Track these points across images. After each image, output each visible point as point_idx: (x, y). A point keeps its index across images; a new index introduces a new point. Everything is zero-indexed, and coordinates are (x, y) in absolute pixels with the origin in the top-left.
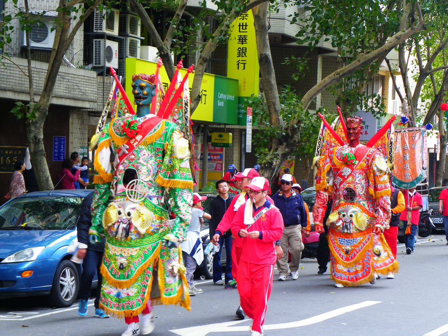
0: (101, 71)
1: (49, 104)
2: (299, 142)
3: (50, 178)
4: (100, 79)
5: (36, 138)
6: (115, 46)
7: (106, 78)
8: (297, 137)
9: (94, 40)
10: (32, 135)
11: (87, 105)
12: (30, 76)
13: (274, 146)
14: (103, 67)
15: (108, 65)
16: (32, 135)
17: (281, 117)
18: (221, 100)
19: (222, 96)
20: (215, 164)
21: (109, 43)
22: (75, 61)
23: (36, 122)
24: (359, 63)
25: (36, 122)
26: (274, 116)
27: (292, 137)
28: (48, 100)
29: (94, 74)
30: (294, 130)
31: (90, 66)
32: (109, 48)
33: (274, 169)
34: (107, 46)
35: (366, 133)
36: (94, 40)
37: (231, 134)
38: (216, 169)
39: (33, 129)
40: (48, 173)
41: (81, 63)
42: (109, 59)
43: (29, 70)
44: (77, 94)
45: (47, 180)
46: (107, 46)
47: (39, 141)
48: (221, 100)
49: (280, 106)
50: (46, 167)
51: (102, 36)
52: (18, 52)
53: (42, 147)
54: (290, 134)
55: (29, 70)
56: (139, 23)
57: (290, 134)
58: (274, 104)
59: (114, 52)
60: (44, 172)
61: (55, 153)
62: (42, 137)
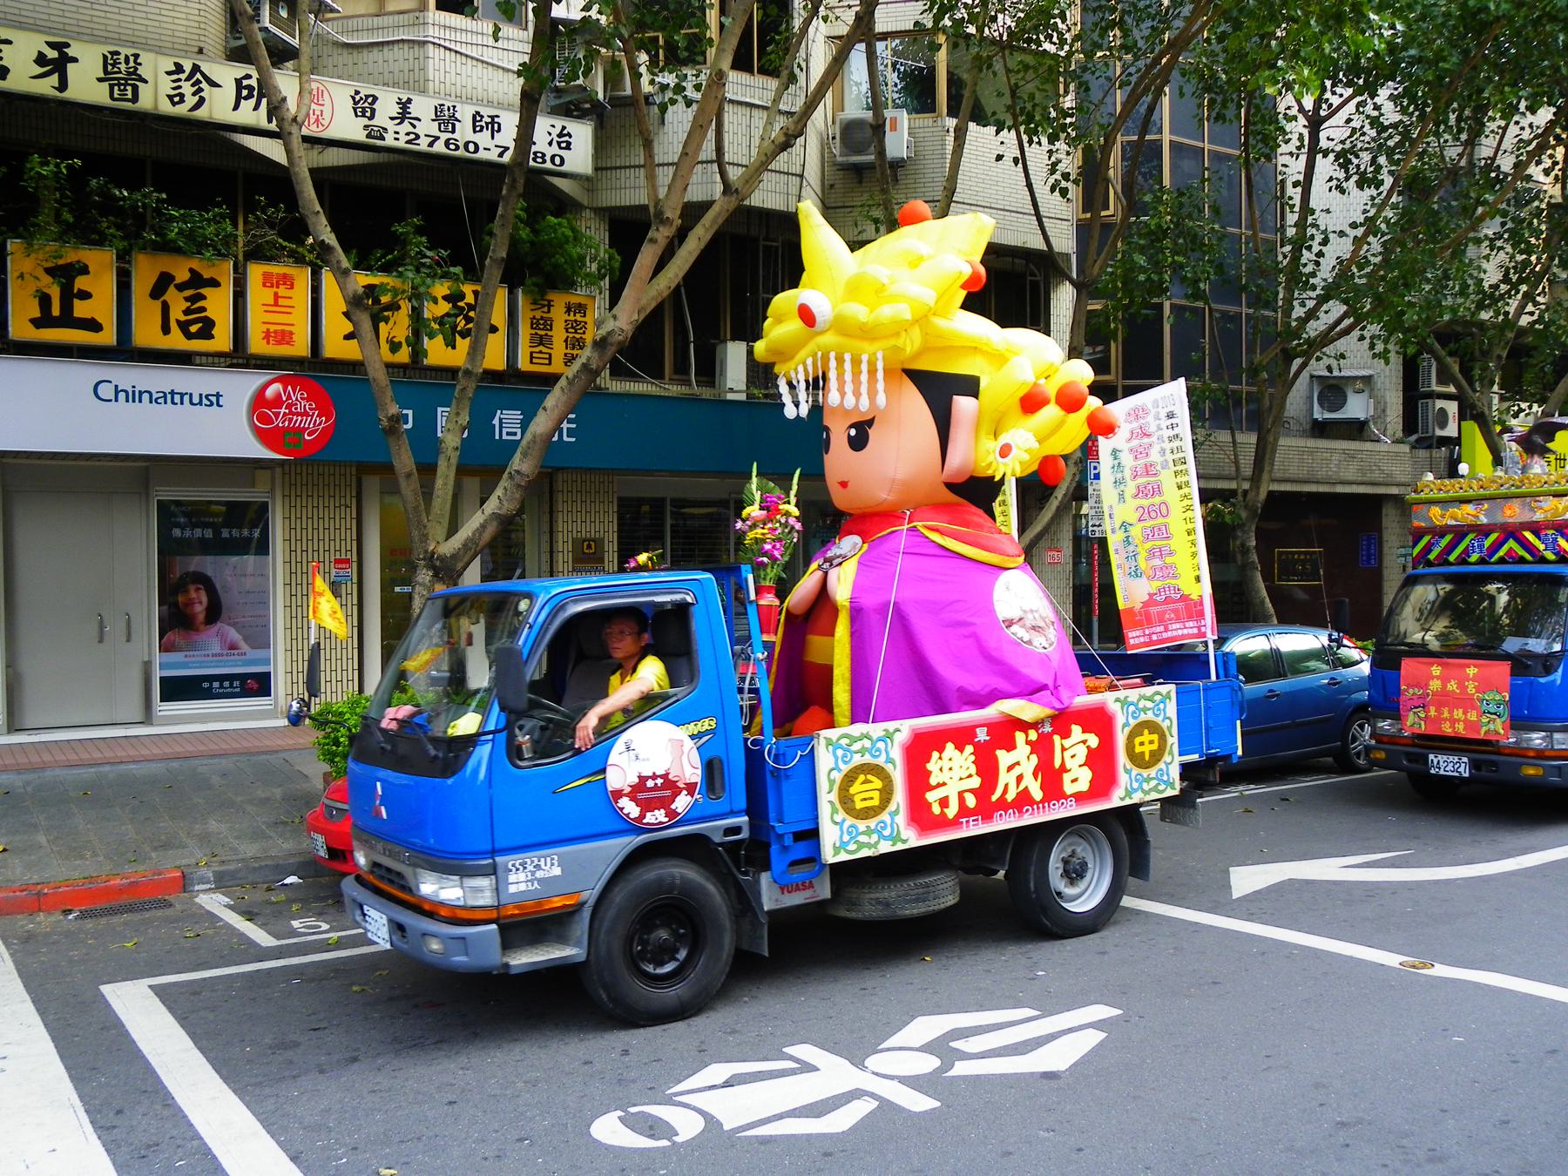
1: (1263, 496)
4: (1422, 453)
5: (1243, 545)
6: (1452, 408)
11: (1394, 491)
12: (1236, 462)
15: (1439, 433)
21: (1440, 404)
22: (1389, 432)
29: (1406, 448)
31: (1413, 438)
32: (1443, 411)
40: (1264, 593)
41: (1400, 434)
42: (1443, 425)
43: (1236, 455)
44: (1376, 476)
45: (1263, 602)
53: (1255, 558)
55: (1236, 455)
60: (1258, 592)
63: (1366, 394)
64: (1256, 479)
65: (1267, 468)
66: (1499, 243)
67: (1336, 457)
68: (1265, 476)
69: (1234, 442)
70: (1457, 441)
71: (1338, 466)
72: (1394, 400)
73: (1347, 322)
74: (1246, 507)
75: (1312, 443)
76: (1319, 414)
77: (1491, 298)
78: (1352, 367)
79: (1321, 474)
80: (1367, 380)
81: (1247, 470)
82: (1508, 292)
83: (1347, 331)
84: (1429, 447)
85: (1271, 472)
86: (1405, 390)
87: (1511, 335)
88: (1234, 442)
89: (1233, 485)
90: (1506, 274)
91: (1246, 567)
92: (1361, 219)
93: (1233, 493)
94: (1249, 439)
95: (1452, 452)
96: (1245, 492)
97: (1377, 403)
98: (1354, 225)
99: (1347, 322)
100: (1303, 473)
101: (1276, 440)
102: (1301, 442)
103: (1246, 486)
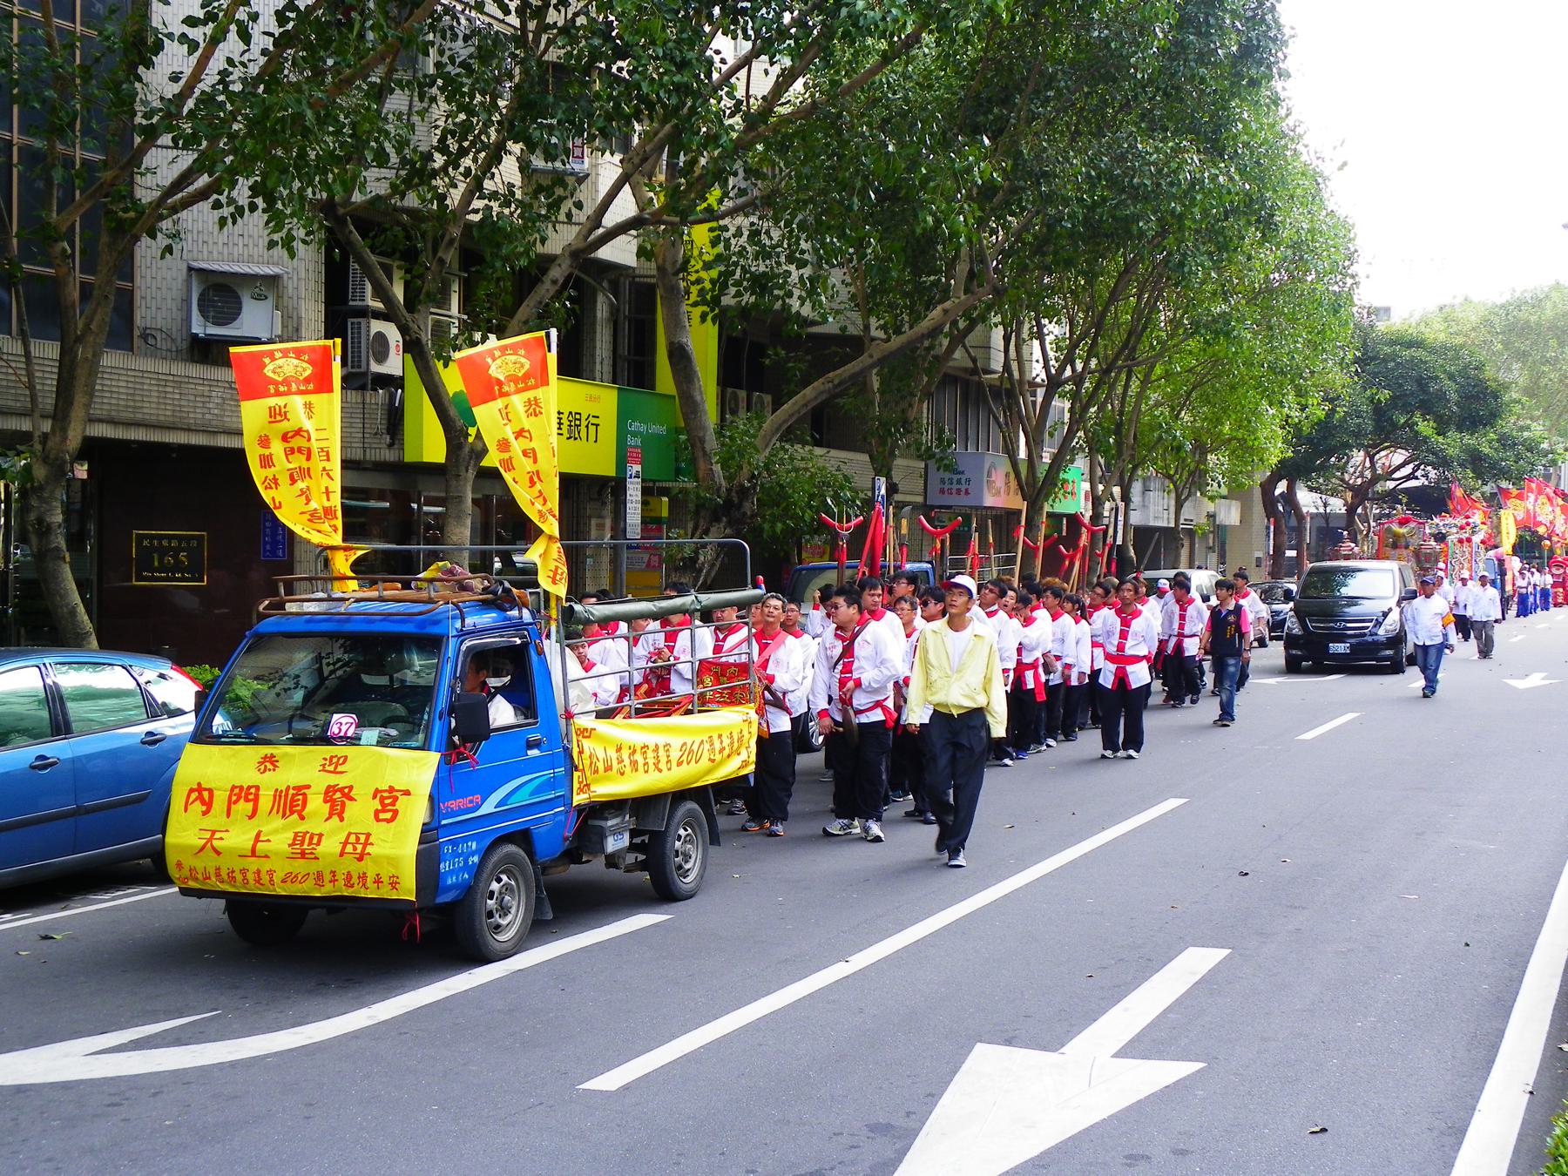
0: (360, 382)
2: (753, 516)
3: (81, 609)
5: (40, 521)
7: (368, 394)
8: (750, 506)
9: (350, 321)
10: (32, 516)
13: (703, 524)
14: (365, 374)
15: (375, 368)
16: (32, 516)
17: (717, 468)
18: (634, 434)
19: (636, 426)
20: (646, 557)
21: (377, 326)
23: (41, 488)
24: (870, 361)
25: (41, 488)
26: (702, 465)
27: (740, 505)
28: (64, 438)
30: (744, 493)
32: (381, 337)
33: (701, 570)
34: (373, 331)
35: (967, 492)
36: (350, 321)
37: (665, 499)
38: (648, 565)
39: (34, 502)
42: (382, 357)
43: (30, 375)
46: (373, 331)
47: (49, 527)
48: (634, 434)
49: (712, 443)
50: (72, 586)
51: (365, 313)
52: (185, 345)
54: (736, 500)
55: (30, 375)
56: (455, 287)
57: (736, 500)
58: (702, 441)
59: (392, 345)
60: (64, 596)
61: (265, 543)
62: (59, 518)
63: (269, 303)
64: (61, 415)
65: (80, 399)
66: (434, 90)
67: (217, 393)
68: (77, 413)
69: (27, 354)
70: (392, 383)
71: (220, 406)
72: (312, 316)
73: (204, 180)
74: (45, 459)
75: (179, 369)
76: (199, 327)
77: (418, 173)
78: (251, 259)
79: (196, 416)
80: (273, 280)
81: (48, 401)
82: (444, 169)
83: (202, 195)
84: (363, 388)
85: (88, 406)
86: (327, 303)
87: (456, 232)
88: (27, 354)
89: (25, 425)
90: (443, 140)
91: (44, 556)
92: (200, 14)
93: (26, 437)
94: (47, 350)
95: (392, 397)
96: (45, 436)
97: (286, 318)
98: (191, 21)
99: (204, 180)
100: (165, 415)
101: (97, 355)
102: (163, 367)
103: (47, 426)
